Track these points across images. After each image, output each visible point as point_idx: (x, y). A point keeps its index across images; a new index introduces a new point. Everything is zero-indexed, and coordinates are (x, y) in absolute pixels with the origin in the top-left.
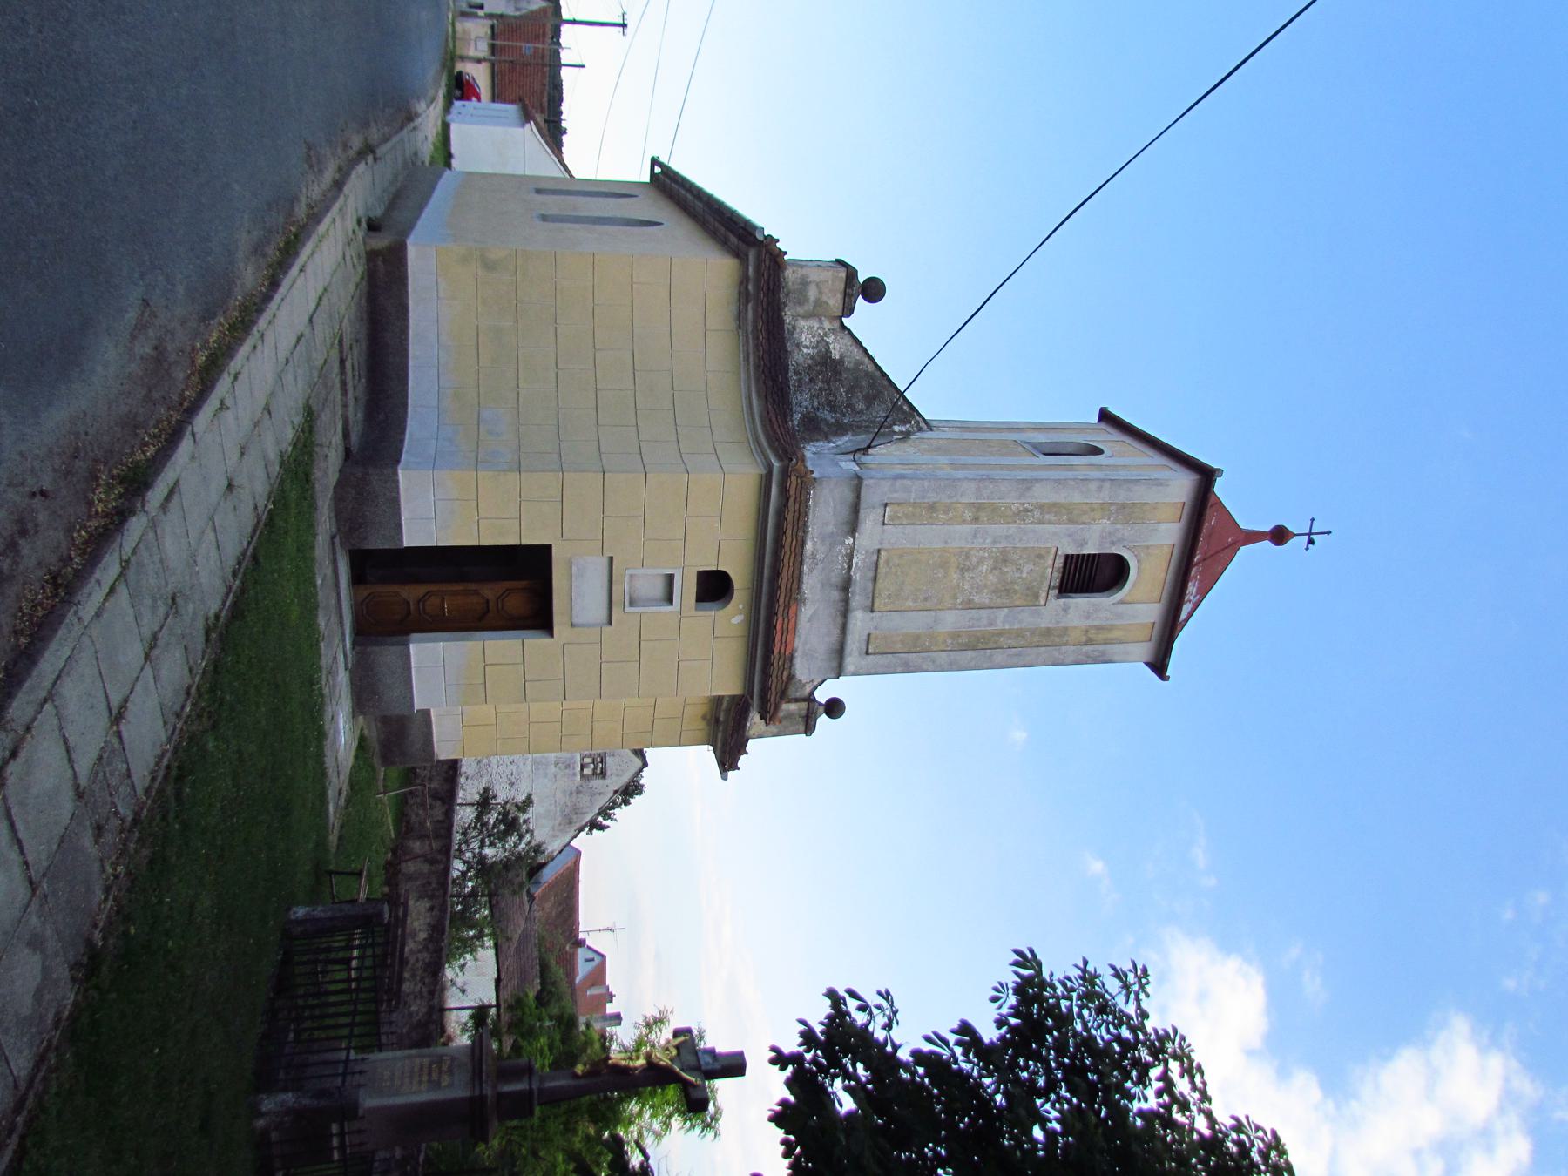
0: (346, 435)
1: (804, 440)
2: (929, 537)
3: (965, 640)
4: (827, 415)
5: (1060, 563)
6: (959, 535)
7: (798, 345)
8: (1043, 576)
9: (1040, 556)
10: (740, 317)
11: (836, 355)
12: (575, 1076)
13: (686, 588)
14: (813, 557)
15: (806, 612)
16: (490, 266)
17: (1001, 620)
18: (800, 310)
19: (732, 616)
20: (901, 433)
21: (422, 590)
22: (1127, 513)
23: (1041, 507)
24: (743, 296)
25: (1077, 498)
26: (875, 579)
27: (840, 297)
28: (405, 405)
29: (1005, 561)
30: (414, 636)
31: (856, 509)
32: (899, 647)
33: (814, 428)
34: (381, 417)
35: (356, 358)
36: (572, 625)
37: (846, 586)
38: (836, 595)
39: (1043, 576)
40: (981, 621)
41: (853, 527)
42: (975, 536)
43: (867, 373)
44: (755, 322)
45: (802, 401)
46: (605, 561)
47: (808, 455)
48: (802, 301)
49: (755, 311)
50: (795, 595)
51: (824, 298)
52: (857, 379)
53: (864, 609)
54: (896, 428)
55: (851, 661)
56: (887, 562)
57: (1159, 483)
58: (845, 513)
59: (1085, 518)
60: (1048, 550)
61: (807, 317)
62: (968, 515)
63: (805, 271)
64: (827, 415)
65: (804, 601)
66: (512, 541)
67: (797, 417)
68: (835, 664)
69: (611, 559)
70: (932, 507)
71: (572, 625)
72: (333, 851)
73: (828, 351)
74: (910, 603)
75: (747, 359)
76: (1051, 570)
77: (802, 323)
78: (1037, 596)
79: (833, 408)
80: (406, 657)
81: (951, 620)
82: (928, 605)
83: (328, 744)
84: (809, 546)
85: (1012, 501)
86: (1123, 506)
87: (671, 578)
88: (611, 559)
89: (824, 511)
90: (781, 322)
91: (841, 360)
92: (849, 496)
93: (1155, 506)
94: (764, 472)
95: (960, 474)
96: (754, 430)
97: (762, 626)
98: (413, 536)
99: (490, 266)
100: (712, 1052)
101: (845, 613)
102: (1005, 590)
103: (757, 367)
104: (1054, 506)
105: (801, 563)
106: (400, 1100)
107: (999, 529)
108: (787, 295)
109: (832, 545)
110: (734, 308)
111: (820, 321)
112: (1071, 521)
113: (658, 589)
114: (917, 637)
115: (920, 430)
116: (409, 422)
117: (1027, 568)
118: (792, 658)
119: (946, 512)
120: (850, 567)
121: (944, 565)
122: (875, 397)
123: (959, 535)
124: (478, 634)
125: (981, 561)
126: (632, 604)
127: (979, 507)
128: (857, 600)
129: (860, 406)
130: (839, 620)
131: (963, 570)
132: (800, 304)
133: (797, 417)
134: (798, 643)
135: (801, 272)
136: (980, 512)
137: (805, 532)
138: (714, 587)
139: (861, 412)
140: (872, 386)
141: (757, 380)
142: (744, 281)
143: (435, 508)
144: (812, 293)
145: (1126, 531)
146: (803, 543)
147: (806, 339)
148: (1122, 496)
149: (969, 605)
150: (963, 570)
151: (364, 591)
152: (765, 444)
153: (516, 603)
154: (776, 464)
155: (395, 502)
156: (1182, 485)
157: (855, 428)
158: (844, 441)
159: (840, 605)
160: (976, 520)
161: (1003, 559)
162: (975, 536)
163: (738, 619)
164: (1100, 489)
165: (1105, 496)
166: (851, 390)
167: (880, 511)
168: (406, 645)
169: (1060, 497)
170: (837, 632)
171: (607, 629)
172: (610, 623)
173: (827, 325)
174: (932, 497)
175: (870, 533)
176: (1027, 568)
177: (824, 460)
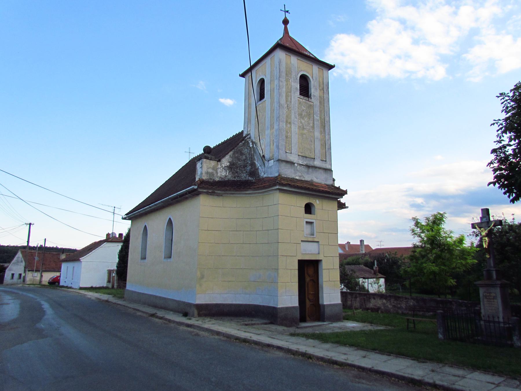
0: (266, 324)
1: (259, 176)
2: (295, 139)
3: (322, 129)
4: (249, 168)
5: (302, 97)
6: (294, 129)
7: (226, 176)
8: (305, 103)
9: (300, 103)
10: (218, 195)
11: (228, 164)
12: (490, 258)
13: (309, 218)
14: (300, 176)
15: (315, 180)
16: (202, 277)
17: (317, 117)
18: (215, 175)
19: (317, 203)
20: (253, 144)
21: (307, 301)
22: (288, 73)
23: (287, 101)
24: (213, 194)
25: (284, 89)
26: (306, 157)
27: (211, 161)
28: (249, 305)
29: (301, 115)
30: (321, 302)
31: (287, 162)
32: (324, 151)
33: (254, 172)
34: (253, 312)
35: (247, 321)
36: (319, 254)
37: (308, 167)
38: (310, 170)
39: (305, 103)
40: (317, 123)
41: (292, 163)
42: (294, 124)
43: (234, 154)
44: (221, 190)
45: (244, 176)
46: (302, 244)
47: (265, 176)
48: (212, 174)
49: (219, 190)
50: (311, 183)
51: (212, 167)
52: (235, 157)
53: (314, 161)
54: (251, 146)
55: (328, 167)
56: (301, 153)
57: (280, 62)
58: (289, 165)
59: (290, 87)
60: (299, 100)
61: (217, 173)
62: (289, 126)
63: (204, 172)
64: (249, 168)
65: (312, 180)
66: (297, 272)
67: (250, 178)
68: (329, 171)
69: (302, 241)
70: (287, 137)
71: (319, 254)
72: (393, 328)
73: (227, 166)
74: (312, 146)
75: (233, 194)
76: (303, 100)
77: (219, 174)
78: (311, 105)
79: (245, 166)
80: (327, 305)
81: (317, 134)
82: (313, 141)
83: (355, 330)
84: (297, 178)
85: (285, 110)
86: (286, 74)
87: (307, 222)
88: (302, 241)
89: (288, 172)
90: (219, 182)
91: (230, 162)
92: (284, 164)
93: (286, 64)
94: (278, 191)
95: (276, 127)
96: (259, 193)
97: (331, 196)
98: (296, 304)
99: (202, 277)
100: (481, 218)
101: (315, 167)
102: (309, 115)
103: (237, 191)
104: (287, 96)
105: (302, 180)
106: (501, 309)
107: (293, 116)
108: (211, 179)
109: (297, 170)
110: (216, 197)
111: (218, 168)
112: (291, 92)
113: (309, 226)
114: (321, 145)
115: (250, 138)
116: (255, 304)
117: (303, 108)
118: (327, 185)
119: (288, 133)
120: (303, 165)
121: (302, 134)
122: (241, 152)
123: (294, 129)
124: (320, 283)
125: (301, 122)
126: (313, 235)
127: (287, 122)
128: (311, 163)
129: (244, 157)
130: (317, 169)
131: (303, 129)
132: (213, 175)
133: (250, 178)
134: (323, 183)
135: (204, 174)
136: (288, 122)
137: (294, 179)
138: (309, 209)
139: (246, 157)
140: (237, 153)
141: (242, 191)
142: (207, 193)
143: (288, 298)
144: (210, 171)
145: (293, 74)
146: (297, 179)
147: (224, 174)
148: (284, 74)
149: (313, 127)
150: (303, 129)
151: (308, 318)
152: (267, 190)
153: (311, 271)
154: (277, 187)
155: (287, 308)
156: (280, 54)
157: (252, 159)
158: (258, 164)
159: (313, 169)
160: (290, 123)
161: (300, 115)
162: (294, 124)
163: (318, 202)
164: (282, 81)
165: (283, 79)
166: (239, 160)
167: (288, 154)
168: (324, 306)
169: (284, 95)
170: (321, 171)
171: (320, 243)
172: (318, 242)
173: (219, 166)
174: (284, 137)
175: (293, 158)
176: (303, 108)
177: (269, 170)
